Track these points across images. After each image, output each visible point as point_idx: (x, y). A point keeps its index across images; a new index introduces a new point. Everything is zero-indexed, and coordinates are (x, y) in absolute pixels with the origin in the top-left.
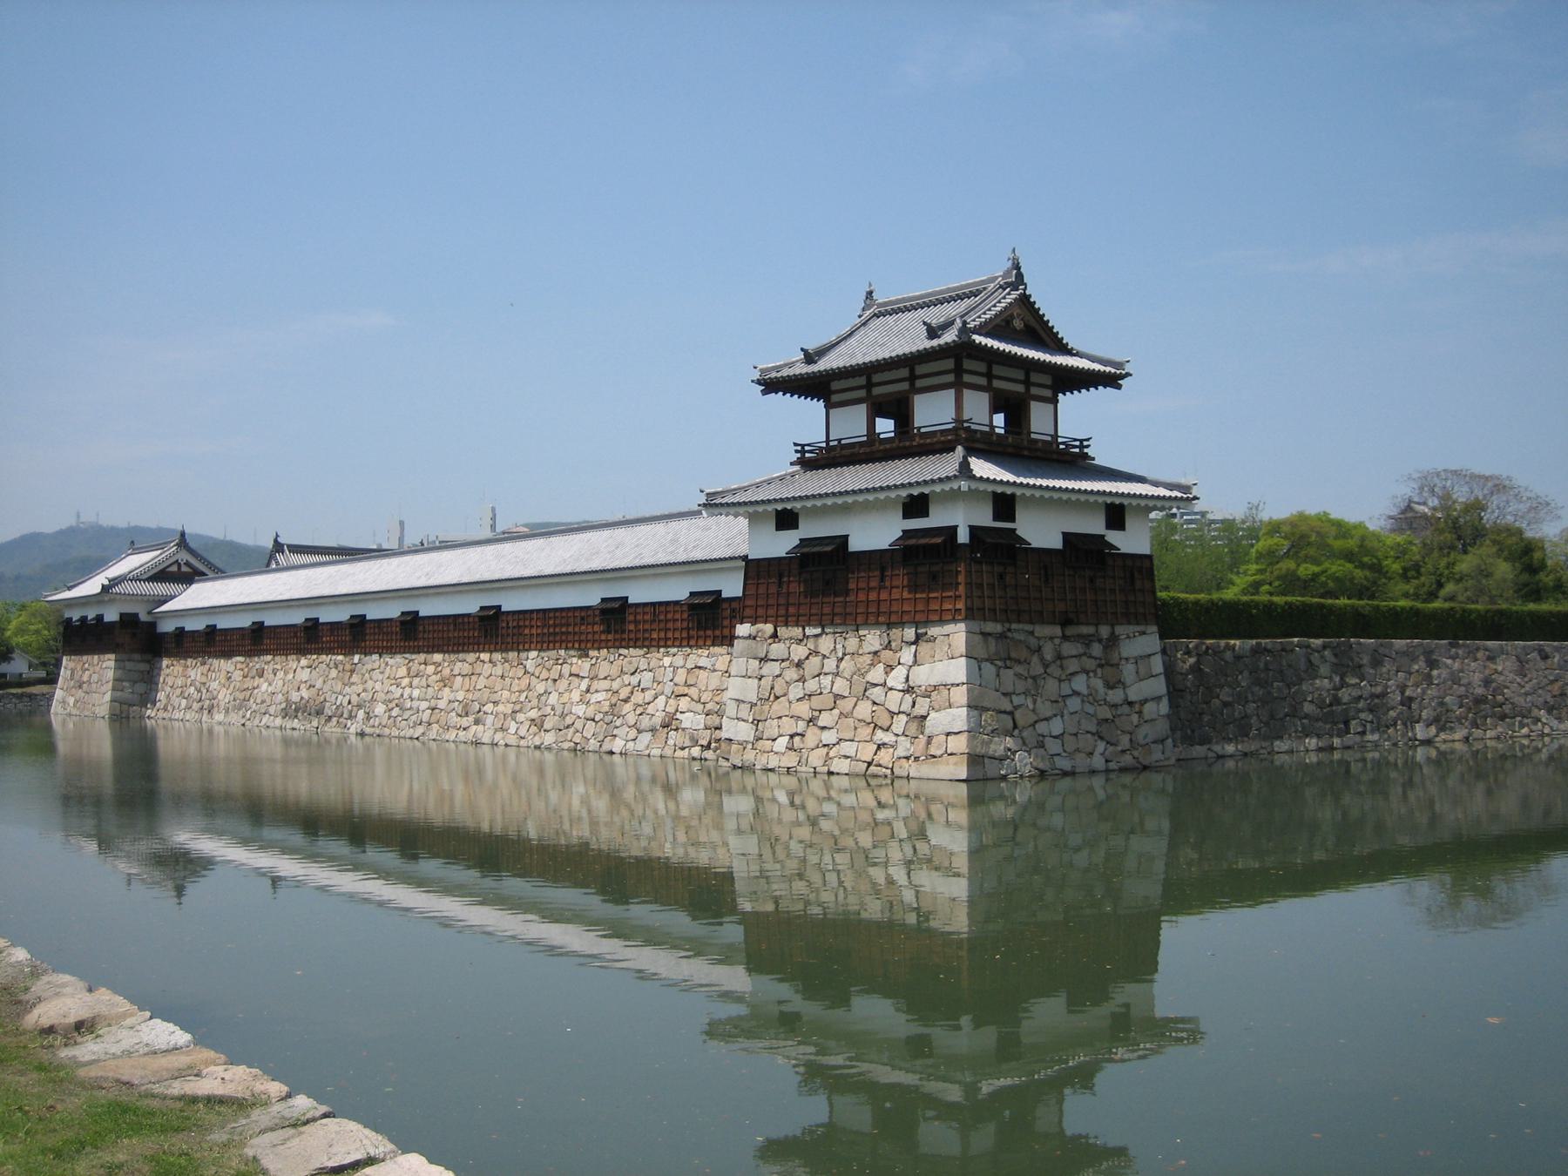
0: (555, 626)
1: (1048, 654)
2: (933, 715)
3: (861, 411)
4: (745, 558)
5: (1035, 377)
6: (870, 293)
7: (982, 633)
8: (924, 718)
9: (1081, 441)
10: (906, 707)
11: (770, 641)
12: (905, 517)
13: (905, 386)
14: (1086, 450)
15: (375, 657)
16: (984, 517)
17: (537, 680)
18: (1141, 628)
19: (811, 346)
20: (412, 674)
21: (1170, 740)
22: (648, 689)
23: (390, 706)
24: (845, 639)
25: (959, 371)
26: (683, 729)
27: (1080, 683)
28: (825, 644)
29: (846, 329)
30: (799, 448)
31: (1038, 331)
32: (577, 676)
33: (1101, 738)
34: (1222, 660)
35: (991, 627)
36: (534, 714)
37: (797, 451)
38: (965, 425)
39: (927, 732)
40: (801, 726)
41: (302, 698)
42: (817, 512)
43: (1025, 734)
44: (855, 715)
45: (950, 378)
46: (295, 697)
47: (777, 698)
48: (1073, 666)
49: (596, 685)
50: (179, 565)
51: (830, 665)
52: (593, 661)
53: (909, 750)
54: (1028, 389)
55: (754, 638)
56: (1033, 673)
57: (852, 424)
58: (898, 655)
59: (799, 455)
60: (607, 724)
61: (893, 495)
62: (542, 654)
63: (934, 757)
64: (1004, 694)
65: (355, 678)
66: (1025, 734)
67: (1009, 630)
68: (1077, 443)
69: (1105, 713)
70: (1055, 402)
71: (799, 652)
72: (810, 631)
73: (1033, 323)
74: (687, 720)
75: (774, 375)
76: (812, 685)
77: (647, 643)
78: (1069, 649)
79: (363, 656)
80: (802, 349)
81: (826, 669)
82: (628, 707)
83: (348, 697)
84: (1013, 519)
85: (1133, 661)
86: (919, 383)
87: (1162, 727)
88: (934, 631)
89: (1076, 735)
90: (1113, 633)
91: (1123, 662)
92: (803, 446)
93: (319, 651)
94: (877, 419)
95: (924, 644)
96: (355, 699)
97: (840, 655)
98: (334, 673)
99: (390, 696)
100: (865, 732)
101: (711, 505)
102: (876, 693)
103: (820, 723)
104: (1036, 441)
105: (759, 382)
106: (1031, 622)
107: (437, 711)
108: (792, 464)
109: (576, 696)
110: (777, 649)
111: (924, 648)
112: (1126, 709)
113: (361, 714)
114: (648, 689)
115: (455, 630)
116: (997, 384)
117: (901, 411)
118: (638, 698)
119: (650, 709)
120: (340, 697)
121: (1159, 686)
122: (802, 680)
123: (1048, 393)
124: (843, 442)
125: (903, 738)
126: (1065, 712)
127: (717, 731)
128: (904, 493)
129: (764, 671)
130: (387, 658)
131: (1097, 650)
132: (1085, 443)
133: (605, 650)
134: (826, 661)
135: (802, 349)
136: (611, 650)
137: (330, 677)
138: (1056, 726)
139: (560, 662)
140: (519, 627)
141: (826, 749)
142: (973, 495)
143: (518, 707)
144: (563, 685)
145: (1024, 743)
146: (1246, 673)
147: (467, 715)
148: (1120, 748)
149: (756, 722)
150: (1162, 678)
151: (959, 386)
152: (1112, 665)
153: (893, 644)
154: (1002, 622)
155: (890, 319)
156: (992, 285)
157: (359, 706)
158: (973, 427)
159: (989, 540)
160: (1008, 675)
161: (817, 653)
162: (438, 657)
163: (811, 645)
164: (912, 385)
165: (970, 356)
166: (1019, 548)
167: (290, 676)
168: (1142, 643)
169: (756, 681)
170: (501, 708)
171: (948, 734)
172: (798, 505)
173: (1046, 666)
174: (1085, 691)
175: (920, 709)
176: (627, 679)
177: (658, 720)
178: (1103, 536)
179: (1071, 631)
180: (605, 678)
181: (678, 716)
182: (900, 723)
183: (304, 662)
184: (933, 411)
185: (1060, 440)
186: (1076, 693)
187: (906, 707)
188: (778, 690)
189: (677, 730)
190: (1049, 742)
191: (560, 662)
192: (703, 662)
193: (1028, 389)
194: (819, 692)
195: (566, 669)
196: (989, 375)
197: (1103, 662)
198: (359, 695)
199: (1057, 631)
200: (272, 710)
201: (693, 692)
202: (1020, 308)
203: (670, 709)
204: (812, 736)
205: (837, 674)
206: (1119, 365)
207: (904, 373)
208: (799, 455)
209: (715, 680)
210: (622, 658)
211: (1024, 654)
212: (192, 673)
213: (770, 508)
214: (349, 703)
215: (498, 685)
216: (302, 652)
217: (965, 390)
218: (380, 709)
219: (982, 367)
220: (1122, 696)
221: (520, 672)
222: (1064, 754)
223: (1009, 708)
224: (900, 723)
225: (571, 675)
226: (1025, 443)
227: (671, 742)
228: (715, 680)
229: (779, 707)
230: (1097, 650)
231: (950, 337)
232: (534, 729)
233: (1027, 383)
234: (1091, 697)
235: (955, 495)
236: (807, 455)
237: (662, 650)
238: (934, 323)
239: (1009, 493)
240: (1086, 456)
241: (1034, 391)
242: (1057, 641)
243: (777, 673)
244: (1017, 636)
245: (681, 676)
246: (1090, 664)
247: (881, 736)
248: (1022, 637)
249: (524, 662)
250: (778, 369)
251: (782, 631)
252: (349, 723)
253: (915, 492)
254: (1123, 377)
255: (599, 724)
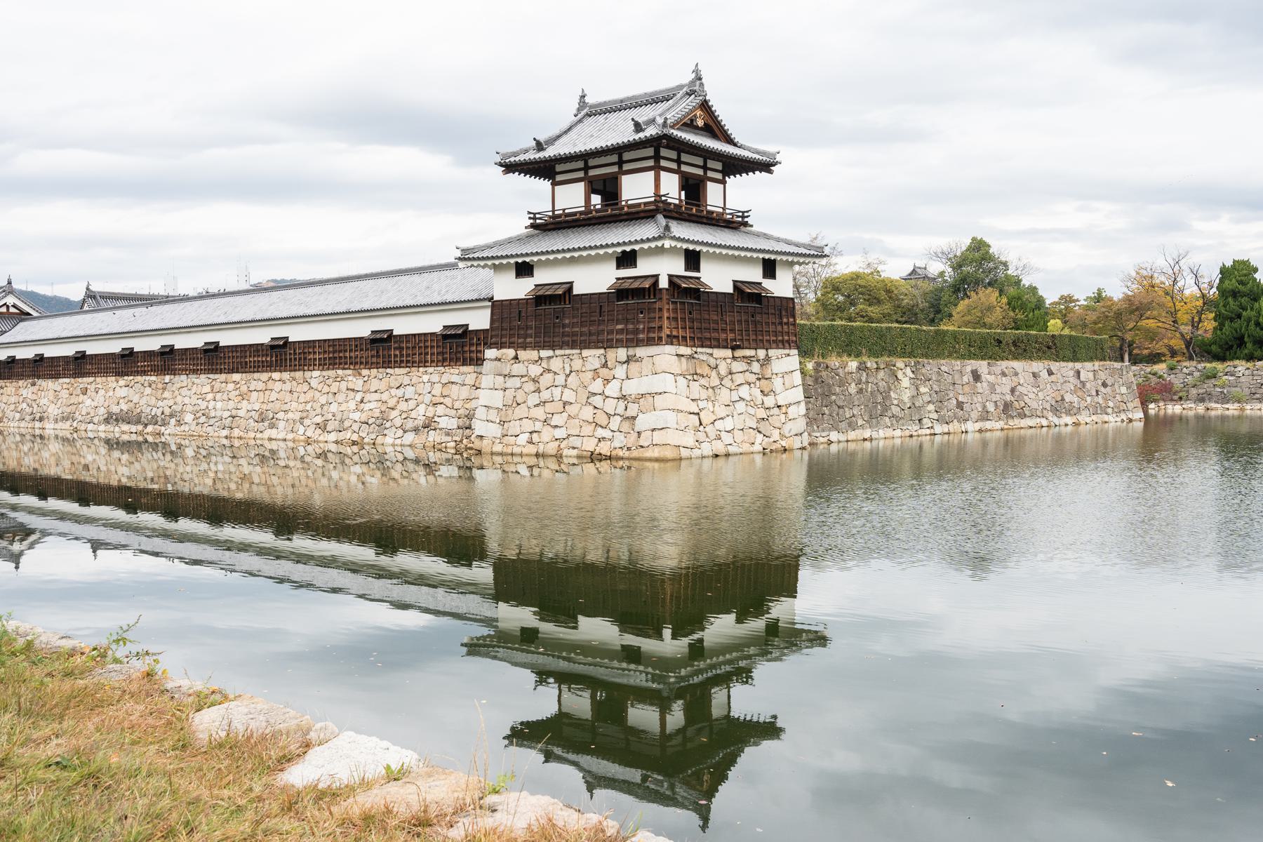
0: (334, 352)
1: (723, 369)
2: (640, 415)
3: (580, 188)
4: (491, 299)
5: (711, 164)
7: (677, 355)
8: (634, 418)
9: (743, 212)
10: (620, 410)
11: (513, 362)
12: (618, 267)
13: (615, 169)
14: (746, 219)
15: (184, 377)
16: (677, 266)
17: (319, 394)
18: (787, 351)
19: (542, 138)
20: (215, 390)
21: (806, 434)
22: (410, 399)
23: (198, 415)
24: (571, 360)
25: (657, 157)
26: (441, 429)
27: (744, 392)
28: (556, 364)
29: (565, 126)
30: (532, 216)
31: (714, 128)
32: (353, 390)
33: (760, 432)
34: (837, 375)
35: (686, 351)
36: (319, 419)
37: (530, 218)
38: (663, 198)
39: (637, 429)
40: (538, 426)
41: (121, 410)
42: (548, 263)
43: (707, 429)
44: (580, 417)
45: (651, 163)
46: (115, 409)
47: (518, 404)
48: (739, 379)
49: (368, 397)
50: (8, 307)
51: (560, 379)
52: (366, 379)
53: (622, 442)
54: (705, 173)
55: (500, 360)
56: (712, 385)
57: (572, 197)
58: (613, 372)
59: (532, 221)
60: (379, 426)
61: (610, 251)
62: (325, 373)
63: (642, 447)
64: (692, 400)
65: (166, 394)
66: (707, 429)
67: (696, 353)
68: (740, 214)
69: (761, 413)
70: (723, 182)
71: (535, 370)
72: (545, 353)
73: (711, 123)
74: (444, 423)
75: (512, 159)
76: (545, 395)
77: (408, 365)
78: (738, 366)
79: (172, 376)
80: (535, 139)
81: (556, 384)
82: (394, 414)
83: (161, 409)
84: (698, 270)
85: (781, 375)
86: (626, 167)
87: (801, 424)
88: (641, 352)
89: (742, 430)
90: (767, 355)
91: (774, 376)
92: (535, 214)
93: (138, 373)
94: (592, 195)
95: (633, 363)
96: (167, 411)
97: (568, 372)
98: (148, 390)
99: (197, 408)
100: (588, 429)
101: (465, 259)
102: (597, 401)
103: (553, 424)
104: (712, 212)
105: (501, 165)
106: (710, 347)
107: (237, 418)
108: (526, 228)
109: (352, 405)
110: (518, 369)
111: (633, 365)
112: (776, 411)
113: (173, 421)
114: (410, 399)
115: (250, 356)
116: (684, 168)
117: (608, 189)
118: (403, 406)
119: (413, 414)
120: (155, 409)
121: (799, 394)
122: (538, 391)
123: (719, 176)
124: (566, 211)
125: (618, 433)
126: (735, 413)
127: (468, 430)
128: (619, 250)
129: (508, 385)
130: (193, 377)
131: (756, 367)
132: (746, 214)
133: (375, 370)
134: (556, 376)
135: (535, 139)
136: (380, 370)
137: (146, 393)
138: (728, 423)
139: (339, 379)
140: (305, 353)
141: (558, 443)
142: (673, 250)
143: (305, 414)
144: (340, 397)
145: (707, 436)
146: (853, 385)
147: (263, 421)
148: (772, 440)
149: (502, 423)
150: (801, 387)
151: (657, 169)
152: (767, 379)
153: (609, 363)
154: (691, 346)
155: (601, 118)
156: (681, 92)
157: (171, 416)
158: (670, 200)
159: (684, 285)
160: (694, 385)
161: (549, 371)
162: (236, 377)
163: (544, 364)
164: (620, 167)
165: (668, 147)
166: (704, 292)
167: (111, 393)
168: (786, 362)
169: (502, 392)
170: (290, 415)
171: (653, 430)
172: (535, 259)
173: (722, 379)
174: (748, 398)
175: (630, 413)
176: (393, 392)
177: (420, 423)
178: (760, 284)
179: (739, 353)
180: (376, 392)
181: (436, 419)
182: (615, 423)
183: (122, 382)
184: (636, 188)
185: (728, 211)
186: (742, 399)
187: (620, 410)
188: (520, 400)
189: (435, 429)
190: (723, 435)
191: (339, 379)
192: (454, 378)
193: (705, 173)
194: (551, 399)
195: (343, 385)
196: (679, 162)
197: (760, 376)
198: (170, 407)
199: (728, 353)
200: (96, 420)
201: (447, 401)
202: (702, 110)
203: (430, 414)
204: (547, 433)
205: (565, 386)
206: (774, 155)
207: (614, 158)
208: (532, 221)
209: (465, 392)
210: (389, 376)
211: (706, 370)
212: (24, 392)
213: (512, 261)
214: (163, 413)
215: (288, 397)
216: (120, 374)
218: (189, 418)
219: (673, 155)
220: (774, 402)
221: (305, 387)
222: (734, 444)
223: (696, 411)
224: (615, 423)
225: (348, 389)
226: (705, 212)
227: (431, 439)
228: (465, 392)
229: (521, 411)
230: (756, 367)
231: (651, 131)
232: (319, 431)
233: (705, 168)
234: (751, 403)
235: (661, 251)
236: (538, 221)
237: (421, 369)
238: (640, 120)
239: (691, 249)
240: (746, 224)
241: (710, 174)
242: (729, 361)
243: (519, 386)
244: (702, 357)
245: (437, 390)
246: (752, 378)
247: (600, 432)
248: (704, 357)
249: (309, 380)
250: (515, 154)
251: (523, 354)
252: (163, 428)
253: (628, 249)
254: (774, 164)
255: (372, 426)
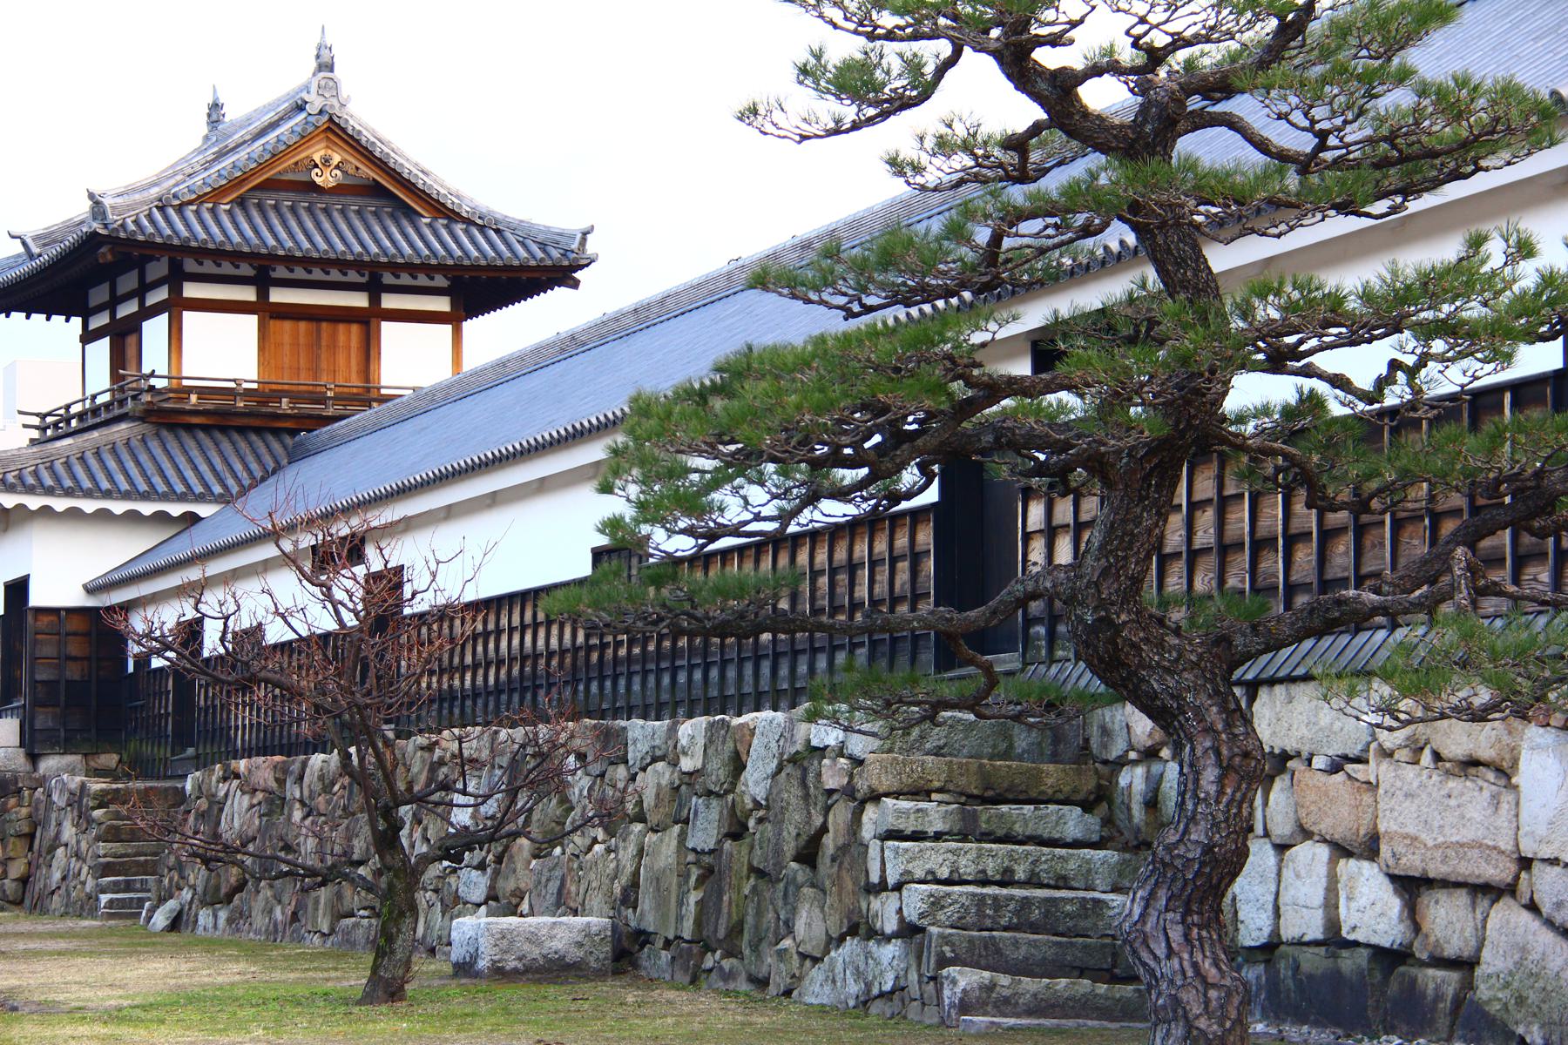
6: (215, 107)
30: (36, 421)
92: (43, 416)
116: (278, 296)
123: (442, 304)
193: (375, 300)
196: (263, 282)
217: (185, 314)
233: (375, 289)
